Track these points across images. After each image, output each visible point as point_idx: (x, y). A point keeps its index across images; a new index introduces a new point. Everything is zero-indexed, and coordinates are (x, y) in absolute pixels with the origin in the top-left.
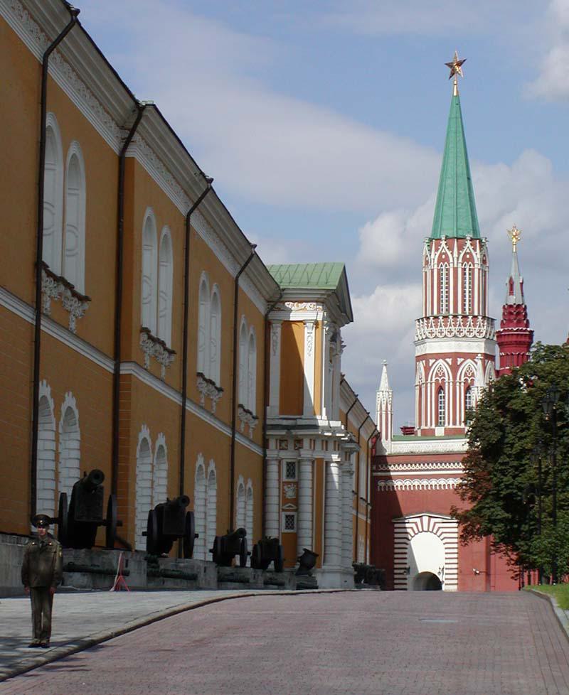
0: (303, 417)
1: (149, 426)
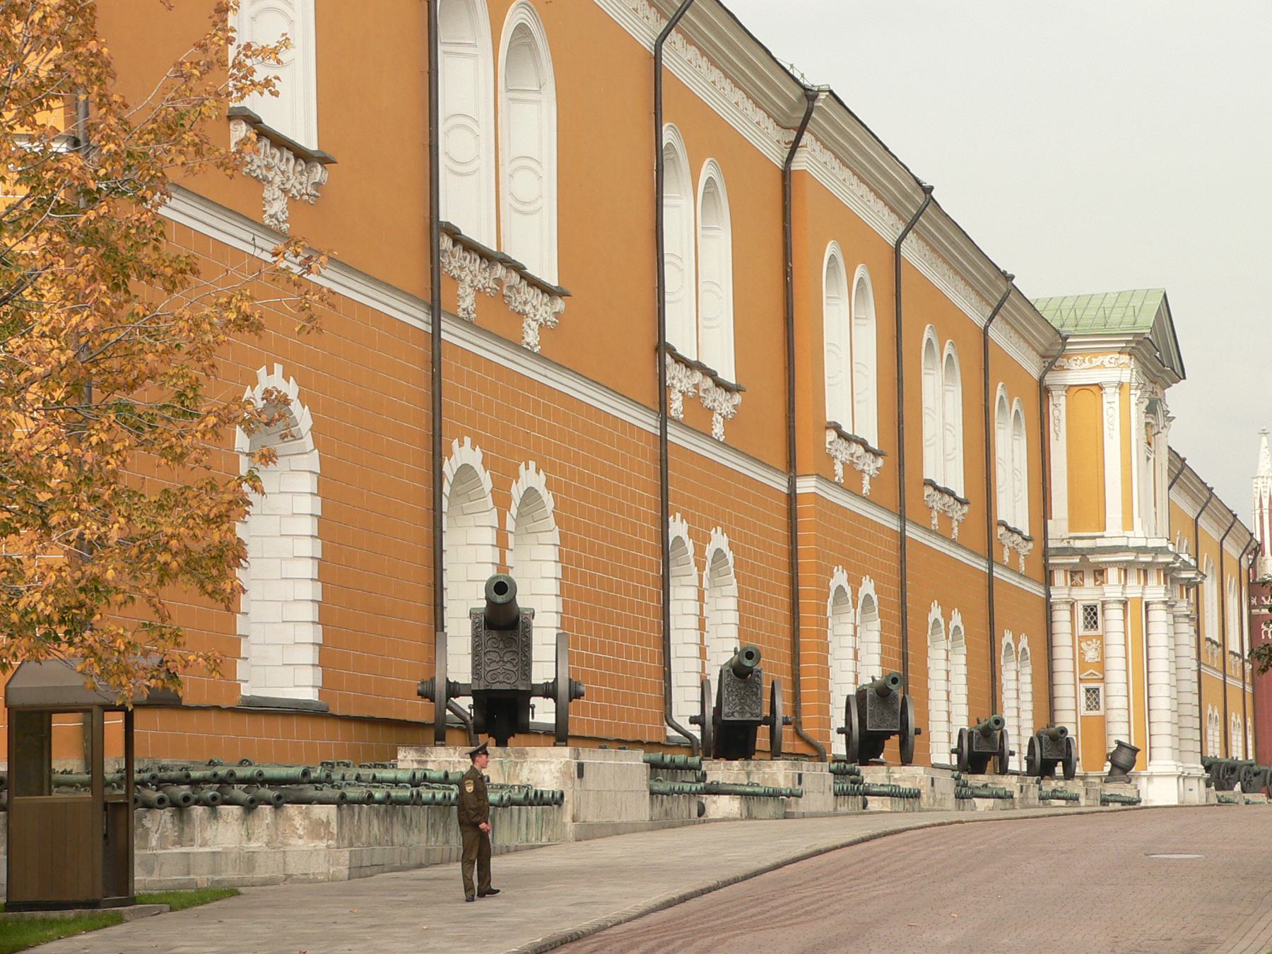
0: (1106, 534)
1: (847, 567)
